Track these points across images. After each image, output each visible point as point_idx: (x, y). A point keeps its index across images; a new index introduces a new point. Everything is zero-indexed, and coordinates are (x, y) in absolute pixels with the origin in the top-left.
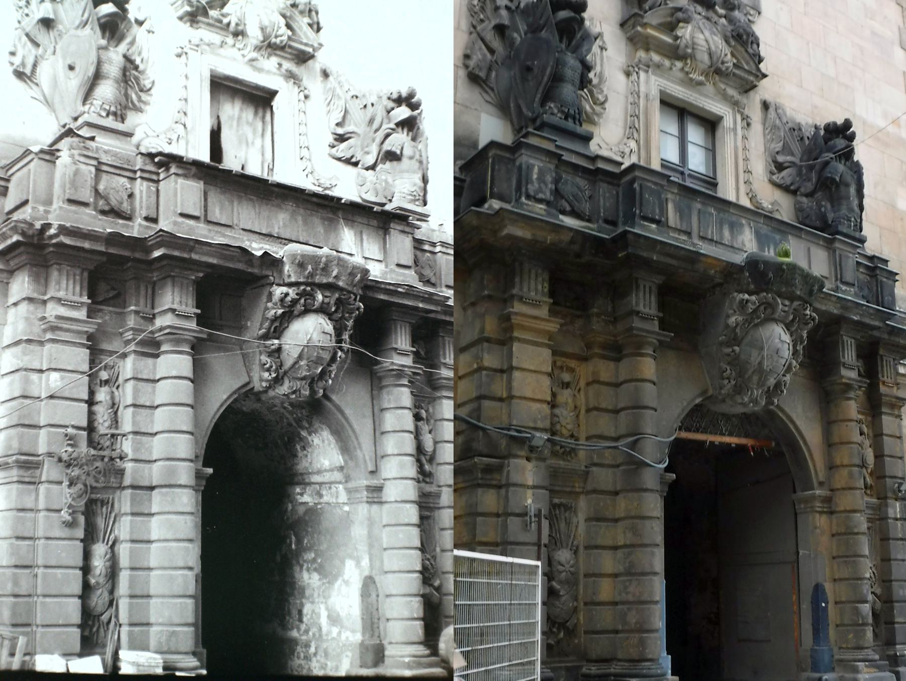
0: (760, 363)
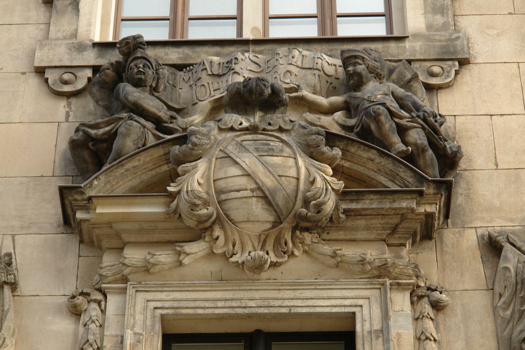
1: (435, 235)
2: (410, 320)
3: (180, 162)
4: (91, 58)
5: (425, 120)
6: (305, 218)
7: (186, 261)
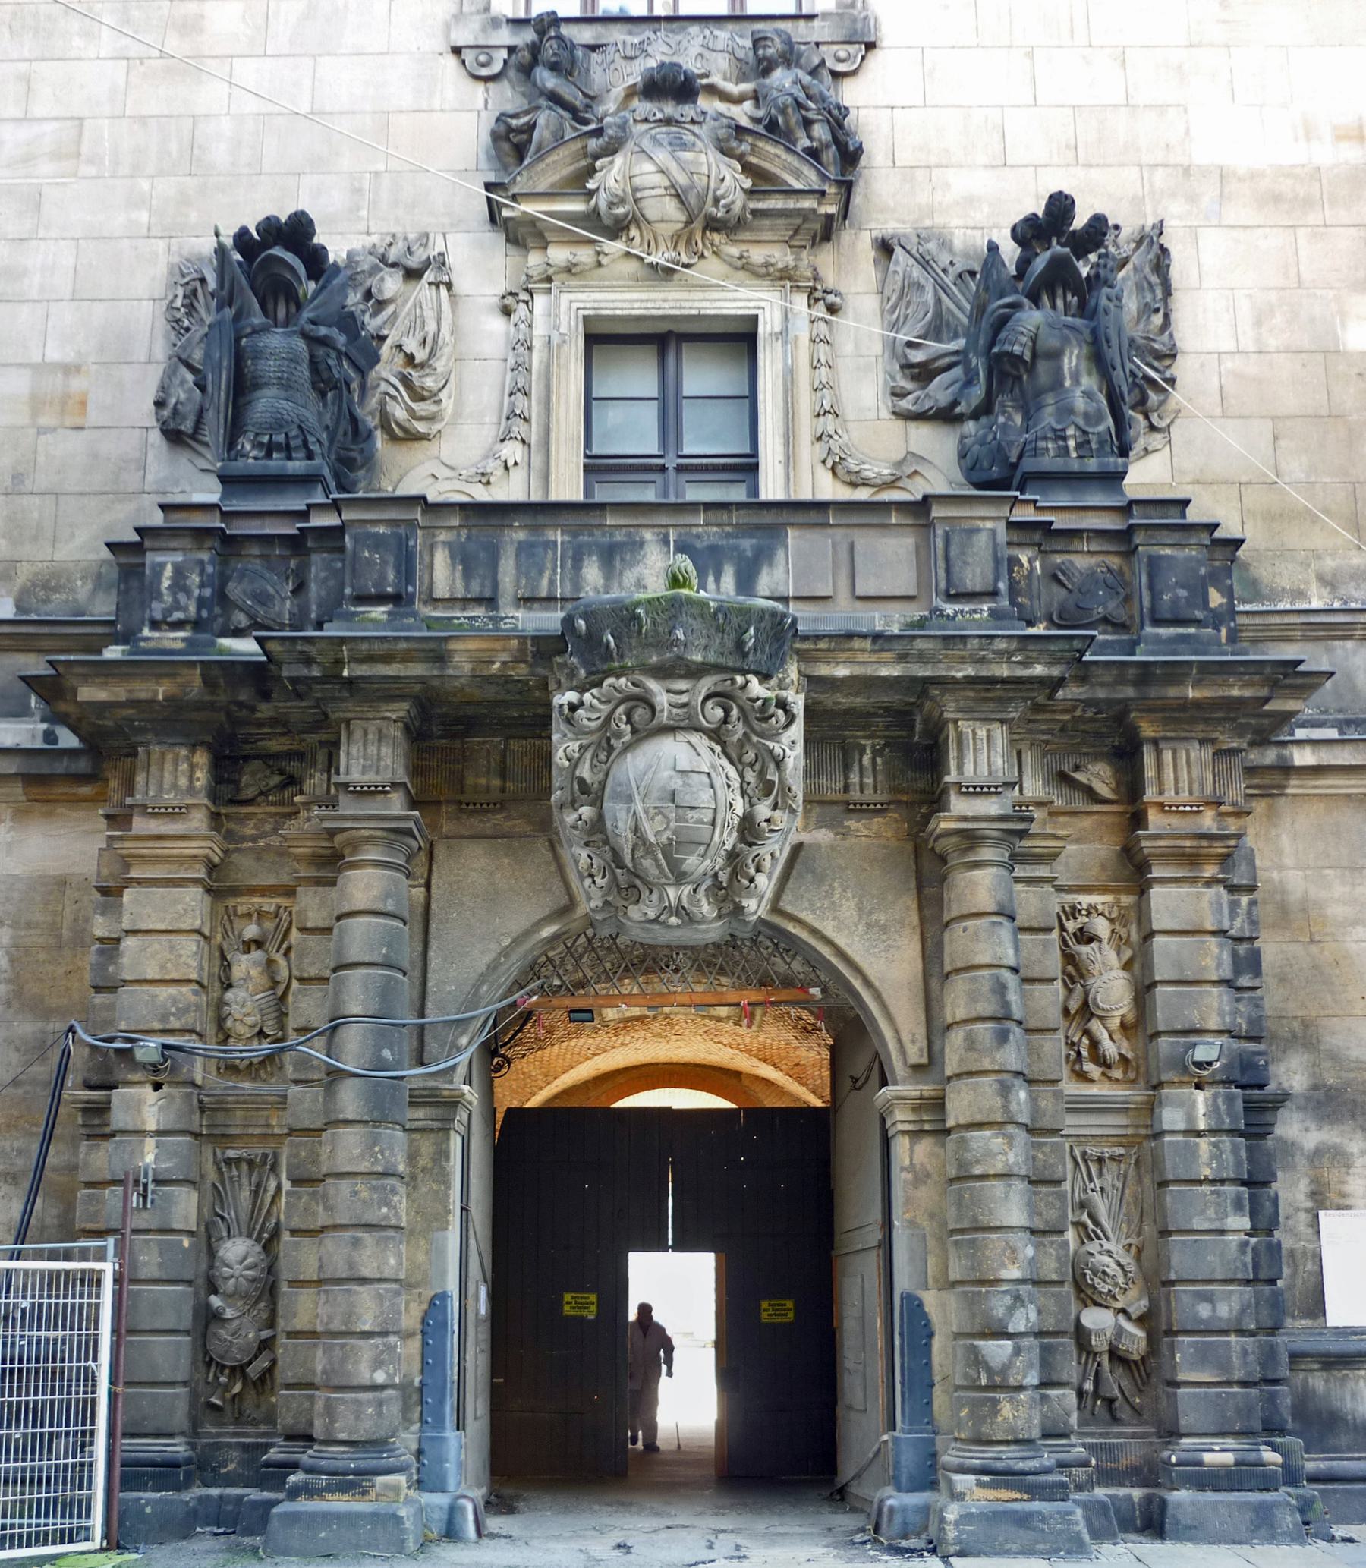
0: (636, 830)
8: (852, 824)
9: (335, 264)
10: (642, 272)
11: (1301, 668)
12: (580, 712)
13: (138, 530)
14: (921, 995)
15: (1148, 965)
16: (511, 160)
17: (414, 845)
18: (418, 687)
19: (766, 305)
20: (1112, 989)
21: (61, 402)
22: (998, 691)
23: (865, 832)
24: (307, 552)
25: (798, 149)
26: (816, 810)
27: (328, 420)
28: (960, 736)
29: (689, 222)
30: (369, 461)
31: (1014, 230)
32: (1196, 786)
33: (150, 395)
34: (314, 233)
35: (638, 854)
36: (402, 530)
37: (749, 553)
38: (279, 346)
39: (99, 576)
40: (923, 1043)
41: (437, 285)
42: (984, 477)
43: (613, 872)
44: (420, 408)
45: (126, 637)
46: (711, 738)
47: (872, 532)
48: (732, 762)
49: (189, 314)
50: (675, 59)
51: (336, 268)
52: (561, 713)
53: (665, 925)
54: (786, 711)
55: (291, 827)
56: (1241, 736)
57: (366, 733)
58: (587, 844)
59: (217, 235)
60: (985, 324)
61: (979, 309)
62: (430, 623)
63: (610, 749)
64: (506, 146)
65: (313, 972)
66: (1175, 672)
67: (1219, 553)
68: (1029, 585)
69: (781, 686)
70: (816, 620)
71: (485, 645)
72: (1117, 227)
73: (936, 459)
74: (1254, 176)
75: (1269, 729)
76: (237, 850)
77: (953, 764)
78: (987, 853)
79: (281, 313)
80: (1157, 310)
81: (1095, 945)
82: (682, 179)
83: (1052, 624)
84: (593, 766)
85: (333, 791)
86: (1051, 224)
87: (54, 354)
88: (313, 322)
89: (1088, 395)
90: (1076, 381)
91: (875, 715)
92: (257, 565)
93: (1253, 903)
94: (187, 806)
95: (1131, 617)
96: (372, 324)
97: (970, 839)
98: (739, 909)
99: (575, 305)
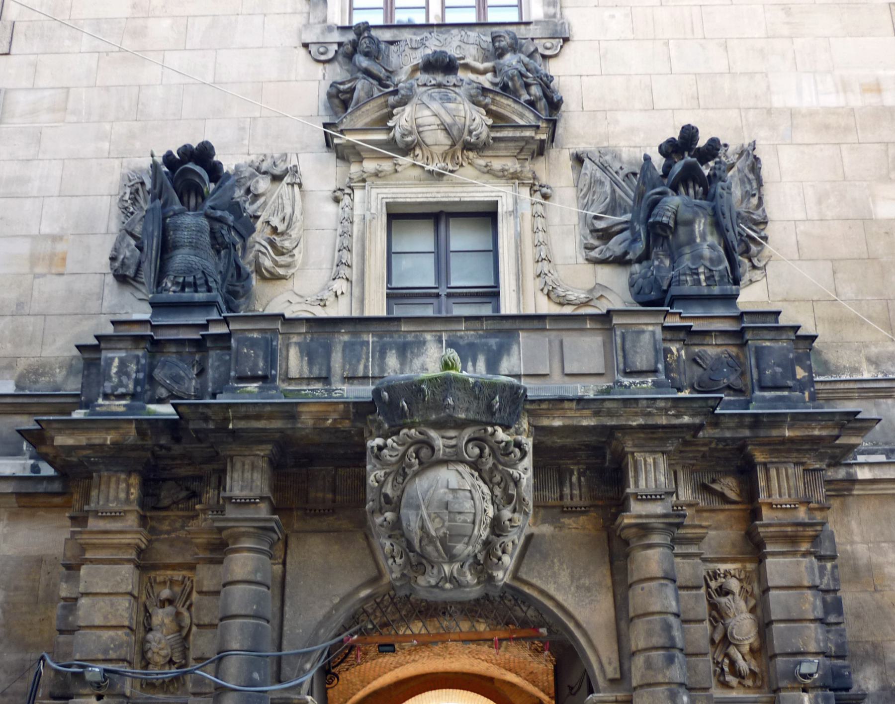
0: (423, 528)
1: (545, 153)
2: (529, 205)
3: (394, 107)
4: (336, 37)
5: (541, 79)
6: (469, 143)
7: (399, 169)
8: (566, 521)
9: (227, 173)
10: (425, 176)
11: (859, 416)
12: (385, 451)
13: (97, 337)
14: (614, 633)
15: (766, 609)
16: (339, 110)
17: (275, 537)
18: (278, 435)
19: (504, 196)
20: (743, 626)
21: (50, 259)
22: (660, 434)
23: (574, 525)
24: (207, 350)
25: (522, 101)
26: (542, 512)
27: (221, 268)
28: (635, 462)
29: (453, 145)
30: (247, 292)
31: (660, 147)
32: (793, 491)
33: (107, 253)
34: (214, 154)
35: (423, 543)
36: (268, 336)
37: (495, 348)
38: (190, 223)
39: (71, 366)
40: (616, 664)
41: (292, 185)
42: (646, 298)
43: (407, 555)
44: (281, 259)
45: (87, 405)
46: (471, 467)
47: (574, 333)
48: (485, 482)
49: (133, 204)
50: (443, 49)
51: (228, 176)
52: (372, 452)
53: (443, 589)
54: (520, 449)
55: (193, 526)
56: (821, 460)
57: (243, 465)
58: (390, 537)
59: (152, 156)
60: (644, 204)
61: (640, 196)
62: (286, 394)
63: (405, 475)
64: (336, 101)
65: (206, 620)
66: (776, 420)
67: (801, 344)
68: (678, 366)
69: (518, 433)
70: (539, 389)
71: (322, 408)
72: (726, 145)
73: (615, 288)
74: (812, 113)
75: (840, 456)
76: (157, 540)
77: (632, 481)
78: (656, 539)
79: (193, 202)
80: (754, 195)
81: (730, 597)
82: (448, 120)
83: (693, 390)
84: (393, 486)
85: (221, 502)
86: (683, 144)
87: (46, 229)
88: (212, 208)
89: (711, 247)
90: (704, 238)
91: (580, 449)
92: (174, 358)
93: (835, 567)
94: (125, 512)
95: (746, 385)
96: (250, 209)
97: (644, 529)
98: (491, 578)
99: (380, 196)
